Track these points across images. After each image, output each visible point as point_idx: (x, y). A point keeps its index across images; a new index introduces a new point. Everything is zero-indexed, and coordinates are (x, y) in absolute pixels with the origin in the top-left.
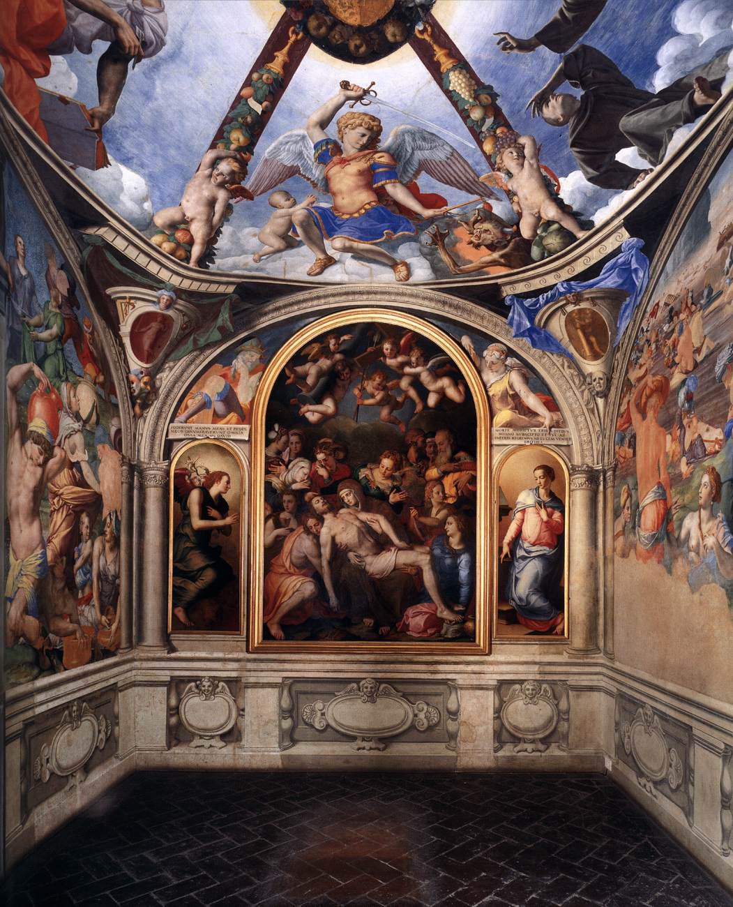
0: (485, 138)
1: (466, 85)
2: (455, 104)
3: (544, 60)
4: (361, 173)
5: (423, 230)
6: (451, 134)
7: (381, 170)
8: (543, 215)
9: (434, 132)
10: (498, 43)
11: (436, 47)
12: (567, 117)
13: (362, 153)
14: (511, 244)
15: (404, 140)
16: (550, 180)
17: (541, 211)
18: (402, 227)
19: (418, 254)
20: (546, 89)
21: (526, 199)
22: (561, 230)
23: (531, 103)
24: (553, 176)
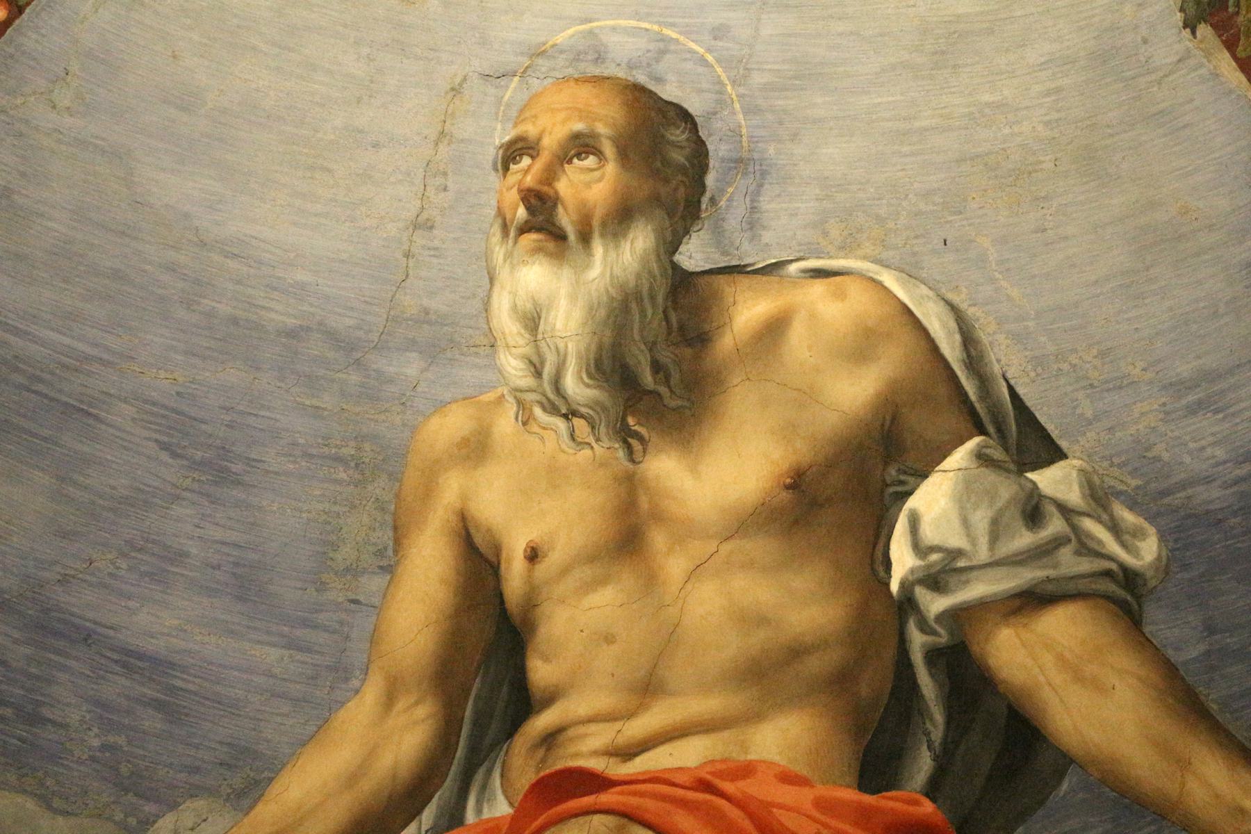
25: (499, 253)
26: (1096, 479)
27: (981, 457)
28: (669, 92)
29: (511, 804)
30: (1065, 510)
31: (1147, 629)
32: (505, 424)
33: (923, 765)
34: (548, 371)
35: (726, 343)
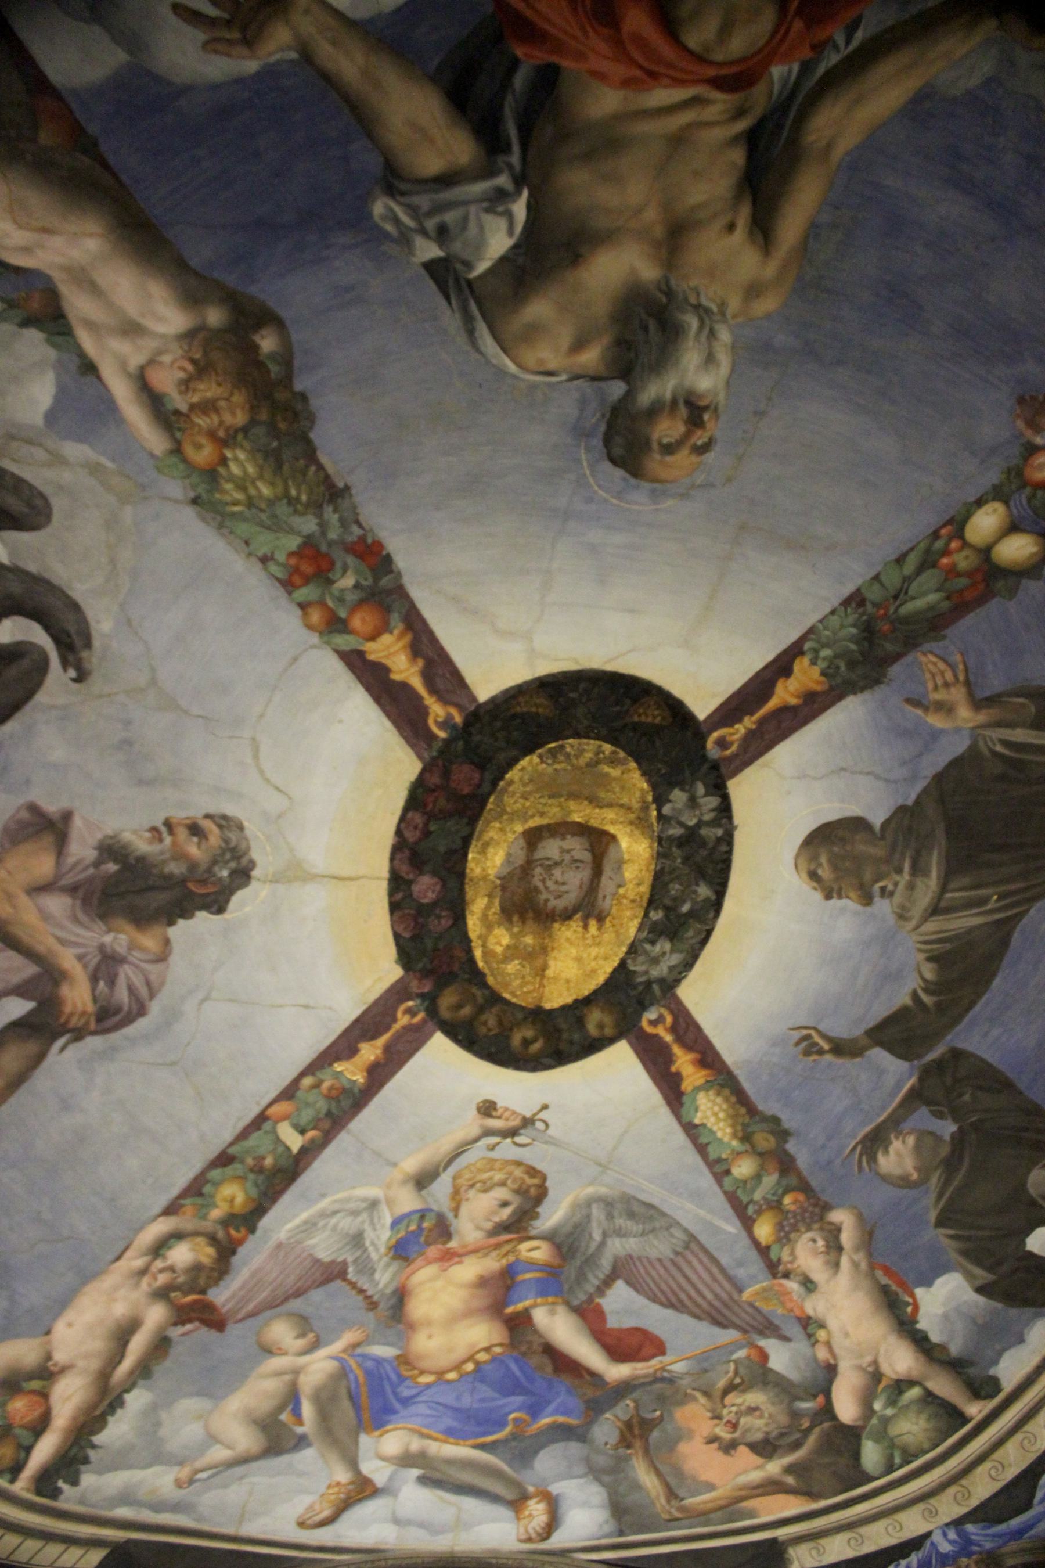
0: (759, 1212)
1: (729, 1116)
2: (702, 1149)
3: (881, 1072)
4: (483, 1282)
5: (602, 1412)
6: (689, 1206)
7: (528, 1276)
8: (885, 1368)
9: (655, 1201)
10: (797, 1044)
11: (677, 1050)
12: (925, 1172)
13: (493, 1241)
14: (812, 1440)
15: (588, 1217)
16: (897, 1294)
17: (881, 1360)
18: (551, 1408)
19: (581, 1469)
20: (884, 1121)
21: (847, 1335)
22: (929, 1397)
23: (854, 1149)
24: (902, 1284)
25: (722, 397)
26: (406, 249)
27: (469, 265)
28: (619, 473)
29: (770, 73)
30: (424, 232)
31: (381, 159)
32: (734, 304)
33: (519, 81)
34: (706, 331)
35: (606, 340)
